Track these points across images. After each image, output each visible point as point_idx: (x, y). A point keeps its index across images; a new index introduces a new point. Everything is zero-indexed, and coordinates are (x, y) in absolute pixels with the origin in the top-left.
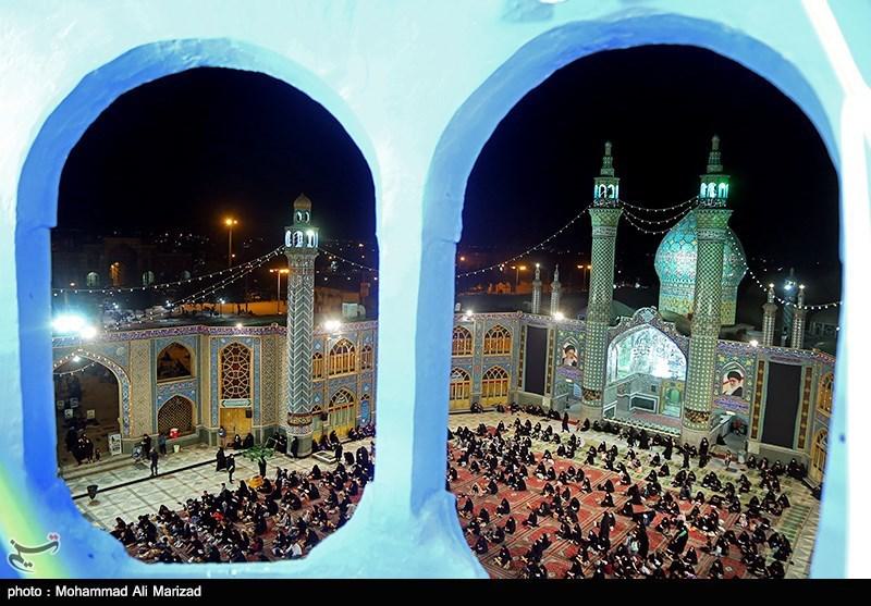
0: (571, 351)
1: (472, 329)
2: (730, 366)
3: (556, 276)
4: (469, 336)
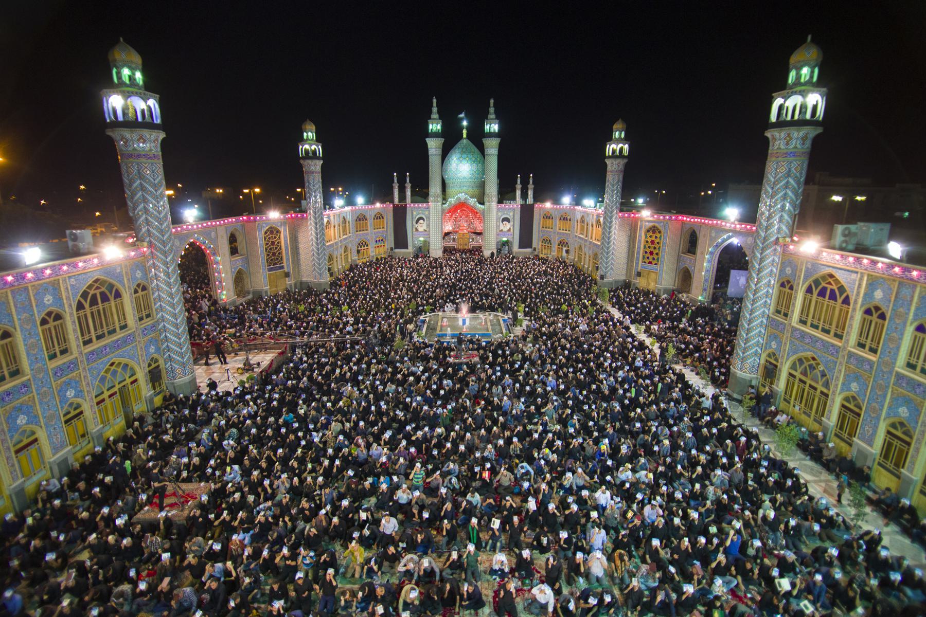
0: (421, 221)
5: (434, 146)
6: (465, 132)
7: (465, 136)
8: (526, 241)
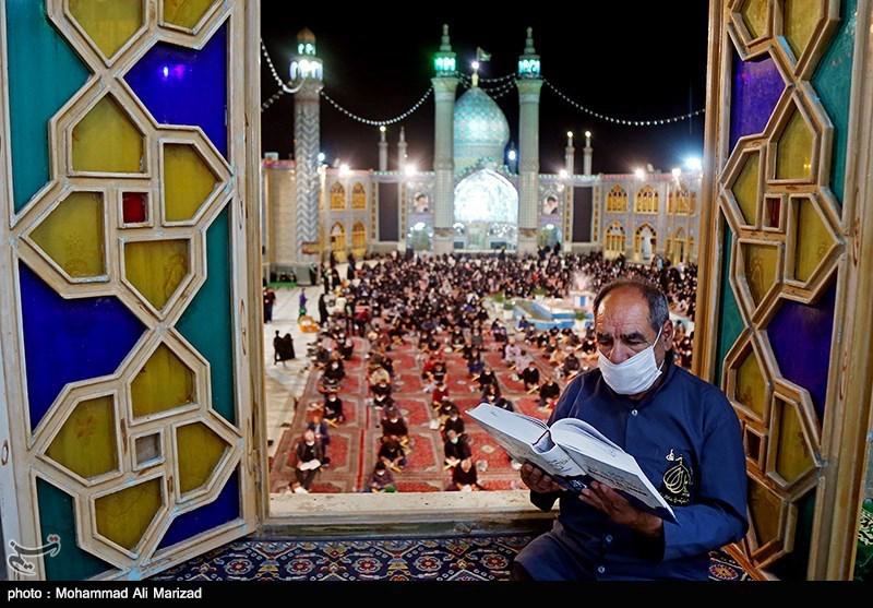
0: (422, 199)
1: (345, 184)
2: (548, 193)
3: (402, 137)
4: (343, 192)
5: (442, 90)
6: (475, 78)
7: (475, 83)
8: (582, 231)
